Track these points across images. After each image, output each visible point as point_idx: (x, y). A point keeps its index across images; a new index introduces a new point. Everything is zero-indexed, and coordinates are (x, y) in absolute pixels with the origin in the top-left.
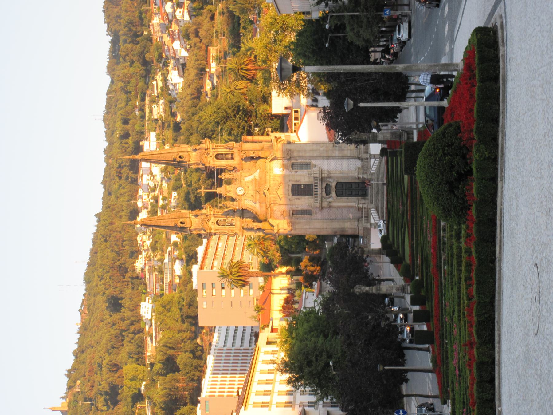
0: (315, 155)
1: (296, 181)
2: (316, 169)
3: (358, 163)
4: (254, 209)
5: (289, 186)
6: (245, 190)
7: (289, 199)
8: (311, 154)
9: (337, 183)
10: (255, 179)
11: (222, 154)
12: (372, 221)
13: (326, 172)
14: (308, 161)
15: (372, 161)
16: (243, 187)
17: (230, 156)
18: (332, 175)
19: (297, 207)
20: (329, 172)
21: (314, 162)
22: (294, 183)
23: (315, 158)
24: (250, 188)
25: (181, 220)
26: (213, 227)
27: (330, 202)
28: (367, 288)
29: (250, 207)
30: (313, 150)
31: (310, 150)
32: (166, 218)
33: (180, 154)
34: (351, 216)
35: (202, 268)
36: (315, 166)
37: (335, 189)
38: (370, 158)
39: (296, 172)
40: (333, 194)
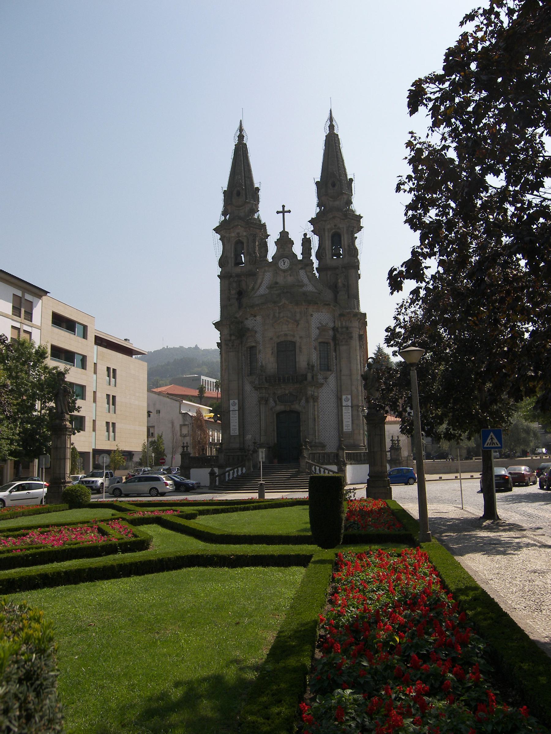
0: (343, 378)
1: (300, 348)
6: (284, 271)
7: (271, 339)
9: (298, 413)
10: (302, 286)
11: (340, 241)
12: (227, 469)
13: (316, 394)
15: (334, 468)
18: (311, 404)
19: (260, 351)
20: (315, 399)
22: (298, 345)
23: (339, 379)
24: (290, 279)
26: (233, 235)
27: (267, 401)
29: (259, 281)
30: (351, 375)
31: (350, 370)
34: (249, 437)
36: (326, 378)
37: (288, 409)
39: (315, 349)
40: (280, 408)
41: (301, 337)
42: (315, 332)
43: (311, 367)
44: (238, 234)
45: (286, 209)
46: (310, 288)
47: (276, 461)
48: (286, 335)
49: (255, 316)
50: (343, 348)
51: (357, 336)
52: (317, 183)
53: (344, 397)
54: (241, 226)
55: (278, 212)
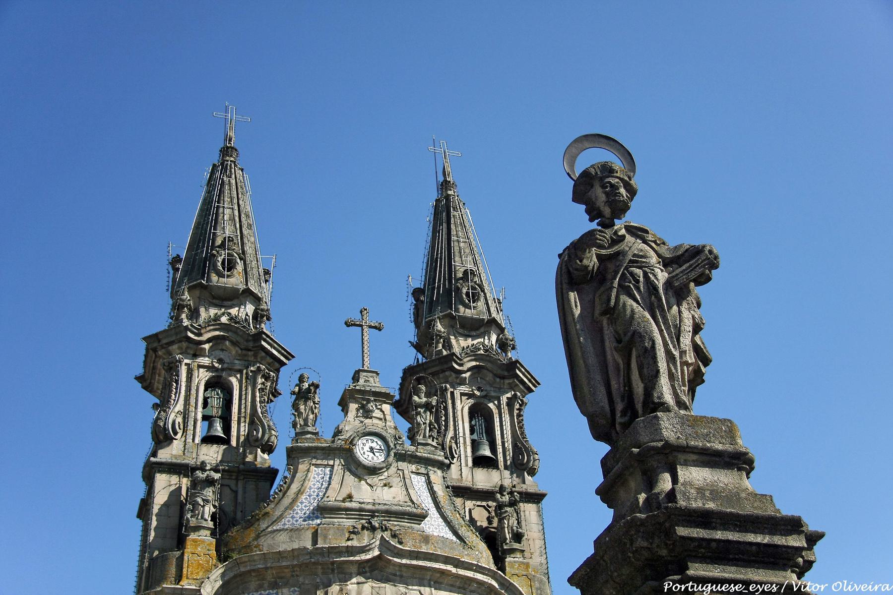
10: (421, 517)
17: (487, 452)
45: (369, 320)
52: (417, 293)
54: (234, 343)
55: (348, 324)
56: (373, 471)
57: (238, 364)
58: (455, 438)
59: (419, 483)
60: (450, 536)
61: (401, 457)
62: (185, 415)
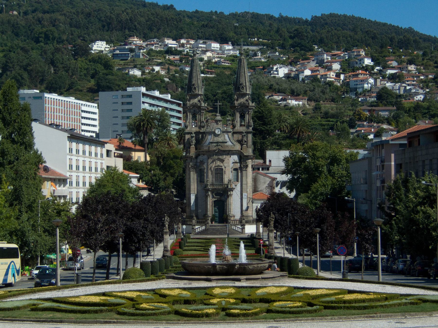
1: (225, 172)
2: (233, 186)
3: (238, 216)
4: (205, 141)
5: (221, 166)
8: (244, 182)
10: (226, 142)
12: (197, 227)
14: (240, 180)
16: (221, 134)
17: (243, 123)
21: (239, 185)
22: (224, 170)
24: (220, 139)
25: (197, 88)
28: (167, 226)
32: (198, 77)
33: (245, 88)
34: (200, 211)
35: (144, 95)
36: (236, 186)
38: (242, 226)
41: (225, 167)
42: (231, 165)
43: (230, 181)
44: (194, 111)
46: (229, 143)
47: (214, 222)
48: (219, 166)
49: (204, 155)
50: (244, 172)
51: (251, 166)
53: (244, 194)
56: (218, 135)
57: (198, 111)
58: (237, 121)
59: (226, 136)
60: (232, 144)
61: (223, 132)
62: (189, 122)
